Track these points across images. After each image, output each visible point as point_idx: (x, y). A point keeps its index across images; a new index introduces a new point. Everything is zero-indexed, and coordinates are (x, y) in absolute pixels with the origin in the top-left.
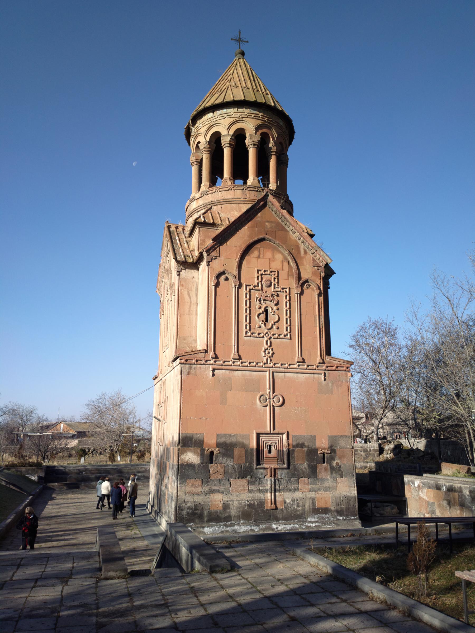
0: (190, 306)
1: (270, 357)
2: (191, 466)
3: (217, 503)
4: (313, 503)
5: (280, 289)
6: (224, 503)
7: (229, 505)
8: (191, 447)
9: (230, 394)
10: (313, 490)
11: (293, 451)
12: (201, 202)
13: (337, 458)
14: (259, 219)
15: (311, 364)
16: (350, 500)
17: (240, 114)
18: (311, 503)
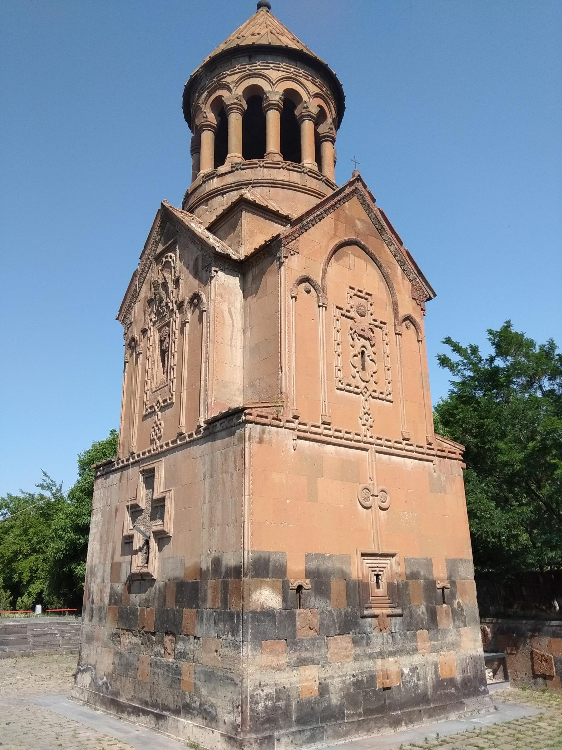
0: (232, 332)
1: (371, 427)
2: (268, 614)
3: (310, 684)
4: (436, 672)
5: (377, 323)
6: (320, 684)
7: (327, 686)
8: (268, 577)
9: (321, 482)
10: (434, 650)
11: (406, 585)
12: (230, 179)
13: (458, 595)
14: (347, 212)
15: (421, 445)
16: (477, 663)
17: (292, 69)
18: (433, 671)
